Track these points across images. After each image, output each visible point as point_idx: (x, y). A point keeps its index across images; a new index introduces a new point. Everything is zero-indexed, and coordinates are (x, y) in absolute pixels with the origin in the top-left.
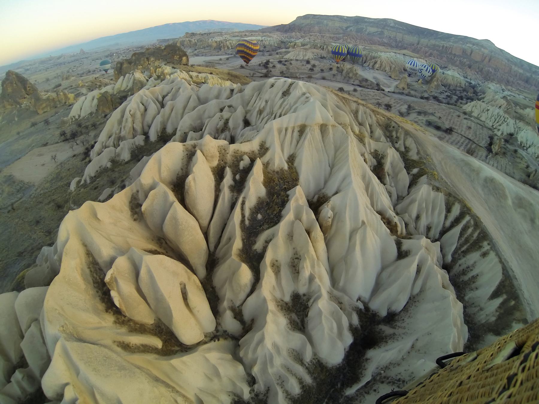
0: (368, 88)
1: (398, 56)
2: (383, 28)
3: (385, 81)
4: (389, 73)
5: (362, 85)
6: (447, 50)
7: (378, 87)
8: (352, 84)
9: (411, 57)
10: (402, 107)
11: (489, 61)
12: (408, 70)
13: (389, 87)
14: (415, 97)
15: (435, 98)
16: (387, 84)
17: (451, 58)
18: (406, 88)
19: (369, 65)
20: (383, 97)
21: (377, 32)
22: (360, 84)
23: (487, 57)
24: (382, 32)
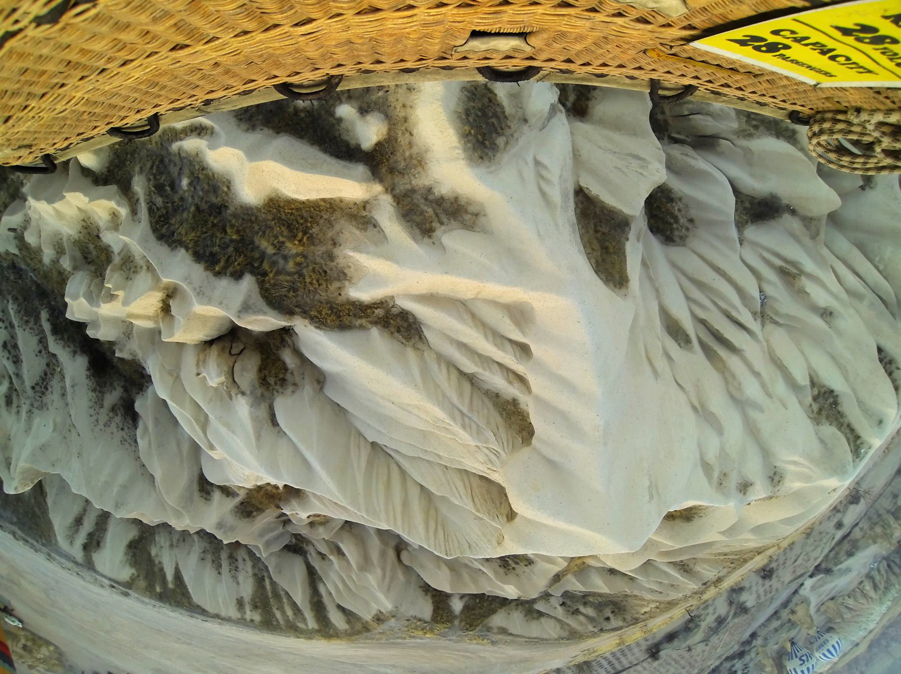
0: (830, 551)
1: (862, 633)
3: (829, 586)
4: (840, 600)
5: (846, 541)
7: (822, 570)
8: (857, 525)
9: (845, 655)
10: (754, 596)
12: (827, 636)
13: (813, 588)
14: (764, 625)
15: (741, 655)
16: (821, 586)
18: (791, 617)
19: (879, 571)
20: (794, 572)
22: (848, 538)
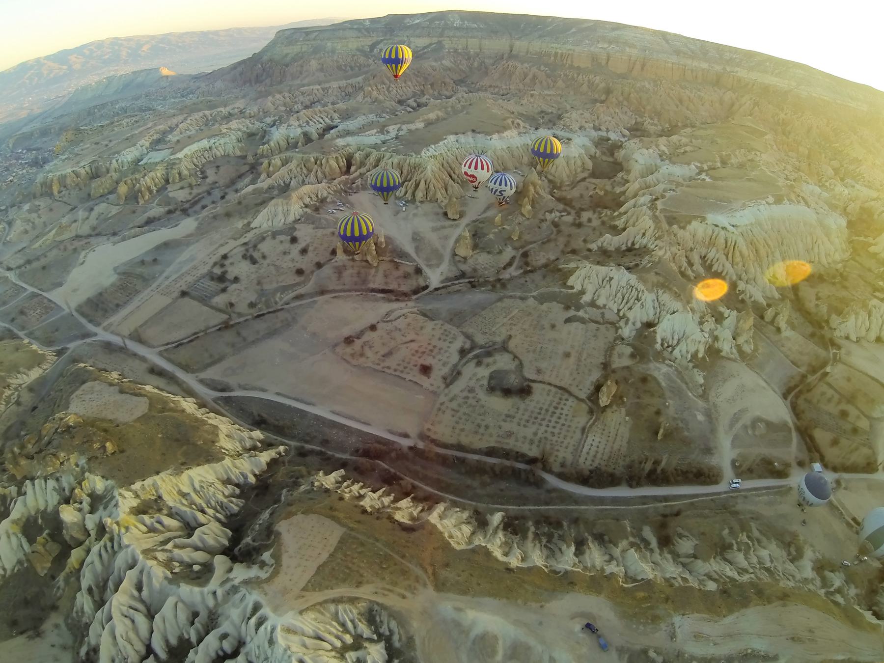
2: (441, 35)
6: (565, 62)
11: (642, 69)
17: (573, 78)
21: (431, 44)
23: (638, 63)
24: (440, 42)
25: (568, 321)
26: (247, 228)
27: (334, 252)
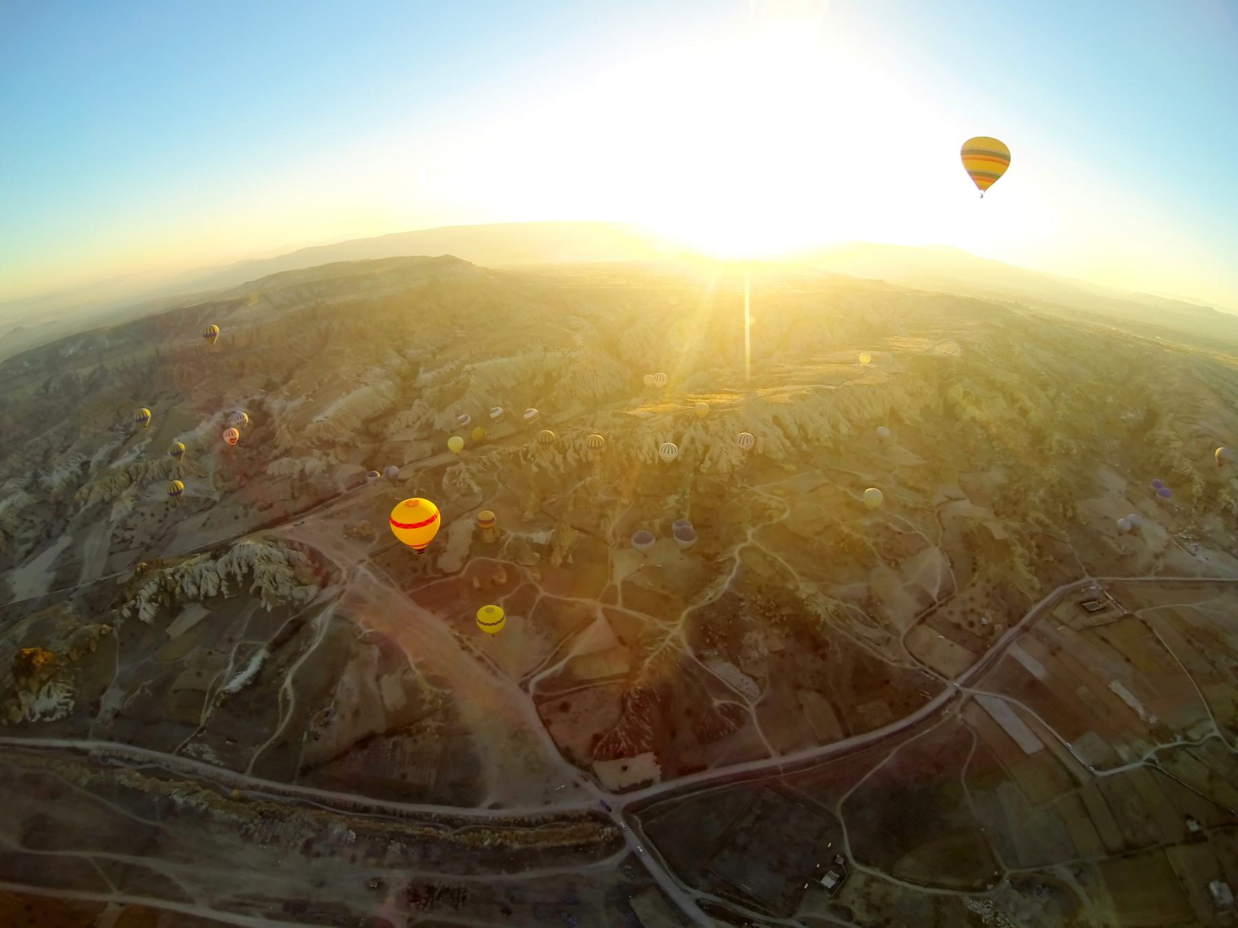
21: (95, 371)
25: (274, 484)
26: (109, 524)
27: (167, 509)
